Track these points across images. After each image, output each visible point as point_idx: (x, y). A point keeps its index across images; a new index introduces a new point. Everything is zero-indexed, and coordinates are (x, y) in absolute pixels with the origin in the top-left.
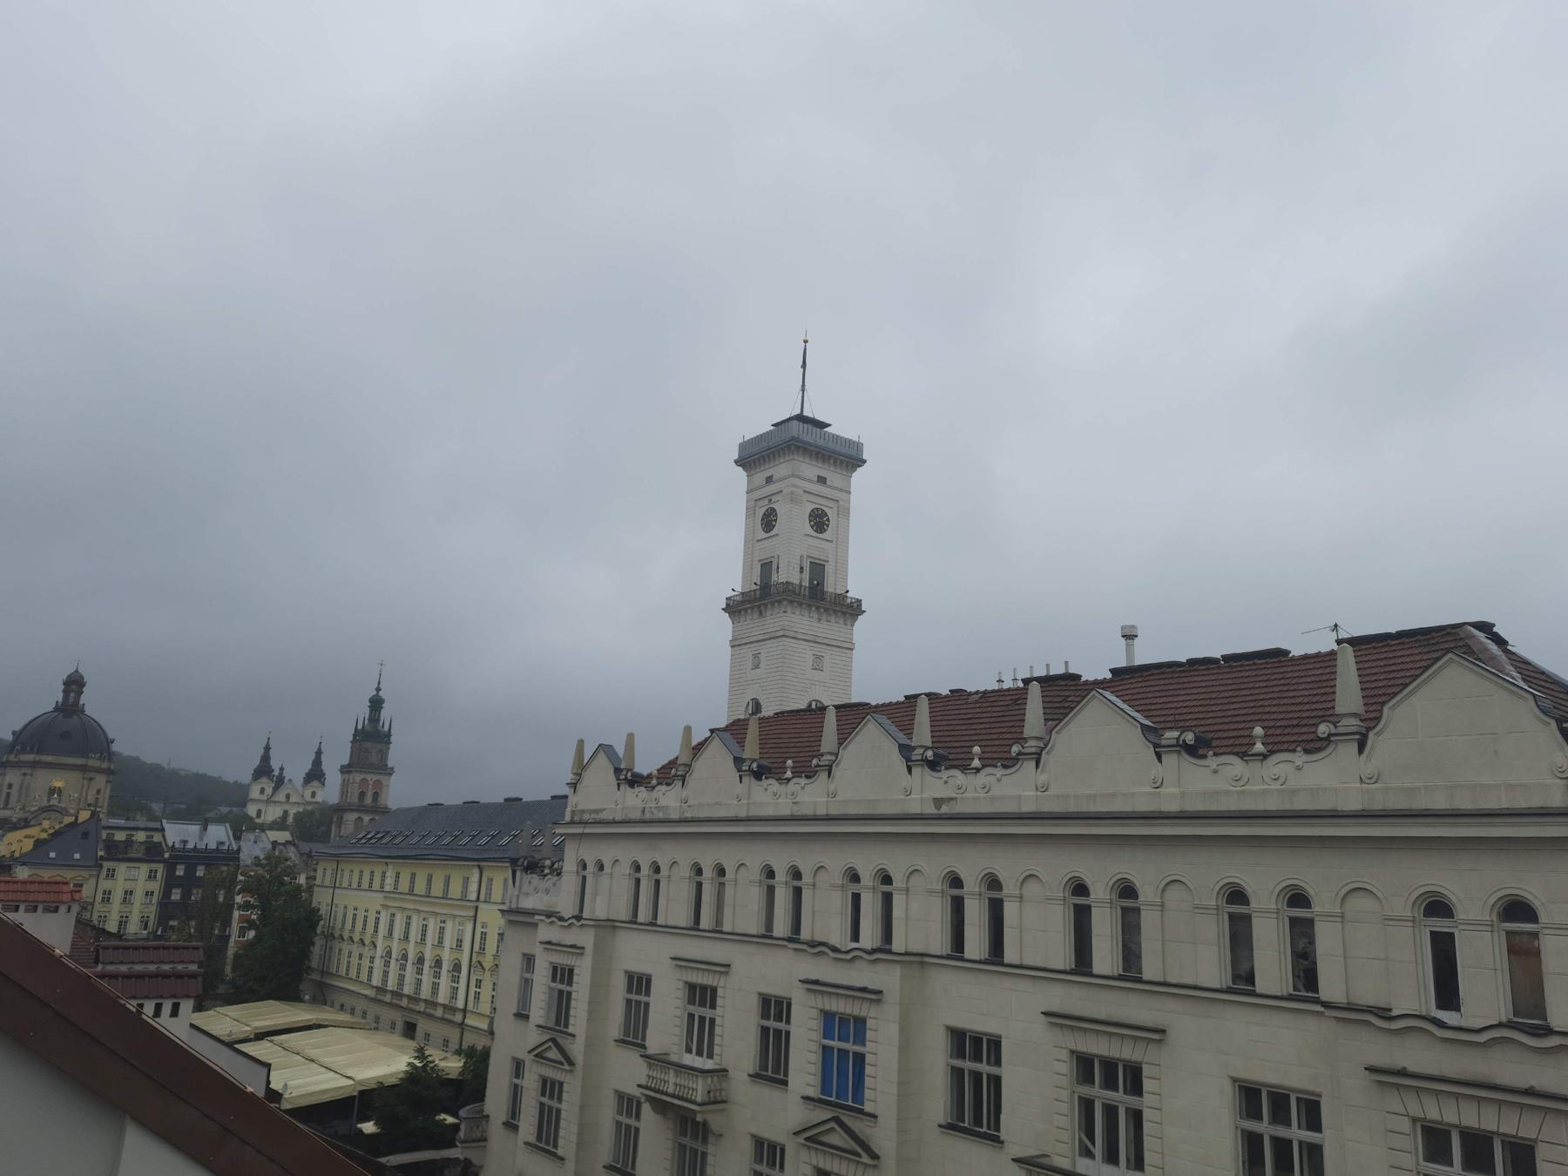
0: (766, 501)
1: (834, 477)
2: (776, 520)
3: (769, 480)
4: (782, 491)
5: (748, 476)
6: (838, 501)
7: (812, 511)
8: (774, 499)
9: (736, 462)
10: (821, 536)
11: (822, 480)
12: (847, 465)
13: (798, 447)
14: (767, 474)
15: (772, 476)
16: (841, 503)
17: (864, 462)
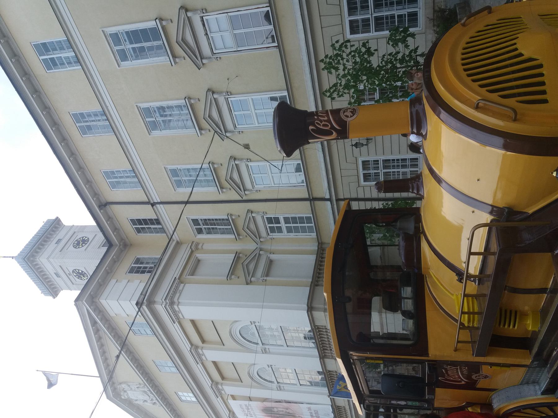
0: (71, 277)
1: (60, 234)
2: (79, 270)
3: (57, 275)
4: (60, 266)
5: (62, 290)
6: (75, 232)
7: (73, 246)
8: (67, 272)
9: (54, 298)
10: (89, 242)
11: (59, 241)
12: (56, 228)
13: (33, 256)
14: (55, 276)
15: (55, 273)
16: (75, 231)
17: (58, 218)
